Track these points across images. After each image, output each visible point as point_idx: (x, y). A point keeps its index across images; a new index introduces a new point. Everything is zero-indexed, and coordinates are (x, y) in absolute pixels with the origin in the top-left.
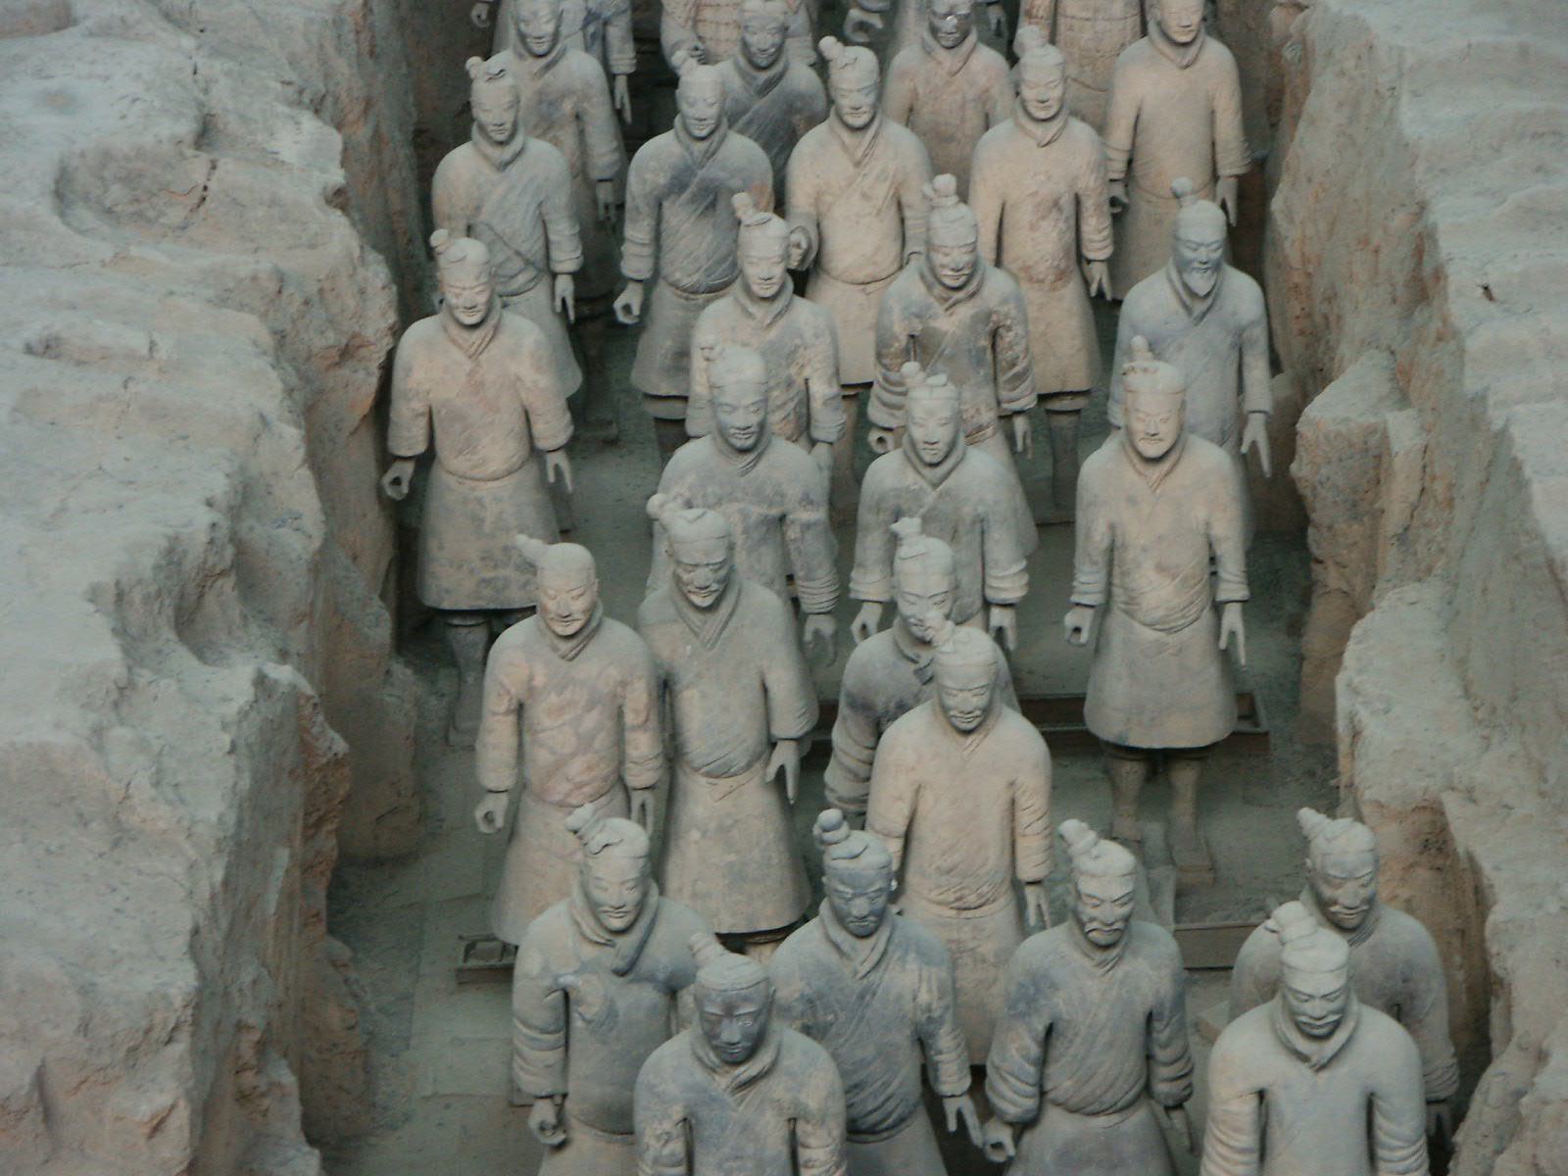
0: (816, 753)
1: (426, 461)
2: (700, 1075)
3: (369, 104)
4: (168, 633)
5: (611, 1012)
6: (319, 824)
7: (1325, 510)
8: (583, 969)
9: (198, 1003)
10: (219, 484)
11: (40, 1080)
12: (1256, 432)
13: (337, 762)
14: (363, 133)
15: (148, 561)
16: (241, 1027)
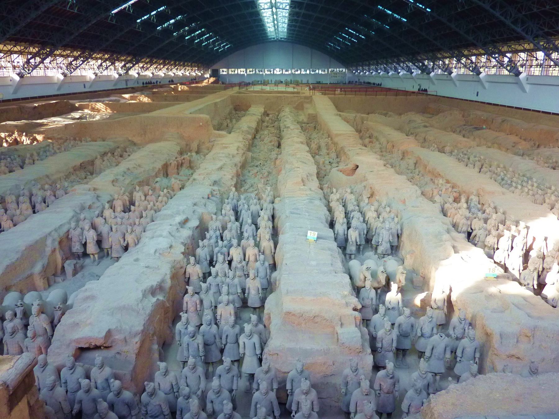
0: (216, 307)
1: (189, 278)
2: (188, 339)
3: (192, 244)
4: (150, 295)
5: (184, 332)
6: (167, 313)
7: (273, 284)
8: (182, 328)
9: (143, 331)
10: (159, 280)
11: (125, 338)
12: (268, 277)
13: (168, 307)
14: (191, 247)
15: (149, 287)
16: (150, 333)
